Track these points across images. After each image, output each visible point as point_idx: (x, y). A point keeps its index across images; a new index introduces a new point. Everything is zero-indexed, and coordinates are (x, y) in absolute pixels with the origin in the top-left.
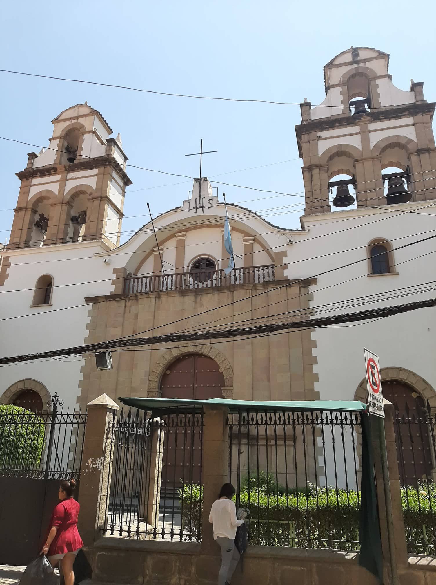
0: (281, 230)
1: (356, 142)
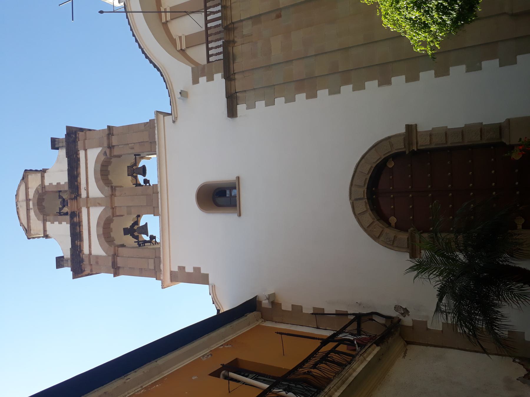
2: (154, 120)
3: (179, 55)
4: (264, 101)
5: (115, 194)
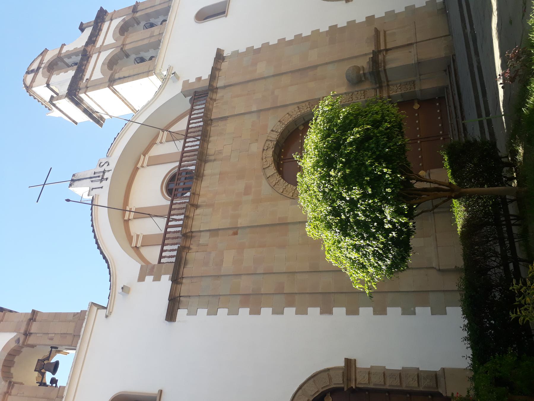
0: (160, 87)
1: (104, 55)
2: (85, 311)
3: (132, 252)
4: (207, 310)
5: (11, 392)
